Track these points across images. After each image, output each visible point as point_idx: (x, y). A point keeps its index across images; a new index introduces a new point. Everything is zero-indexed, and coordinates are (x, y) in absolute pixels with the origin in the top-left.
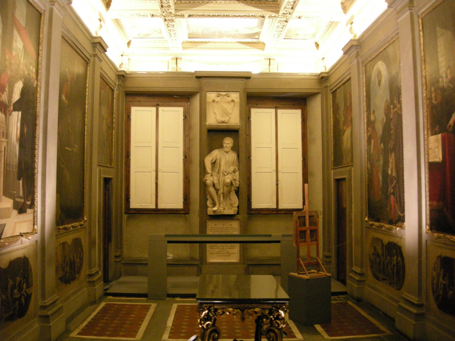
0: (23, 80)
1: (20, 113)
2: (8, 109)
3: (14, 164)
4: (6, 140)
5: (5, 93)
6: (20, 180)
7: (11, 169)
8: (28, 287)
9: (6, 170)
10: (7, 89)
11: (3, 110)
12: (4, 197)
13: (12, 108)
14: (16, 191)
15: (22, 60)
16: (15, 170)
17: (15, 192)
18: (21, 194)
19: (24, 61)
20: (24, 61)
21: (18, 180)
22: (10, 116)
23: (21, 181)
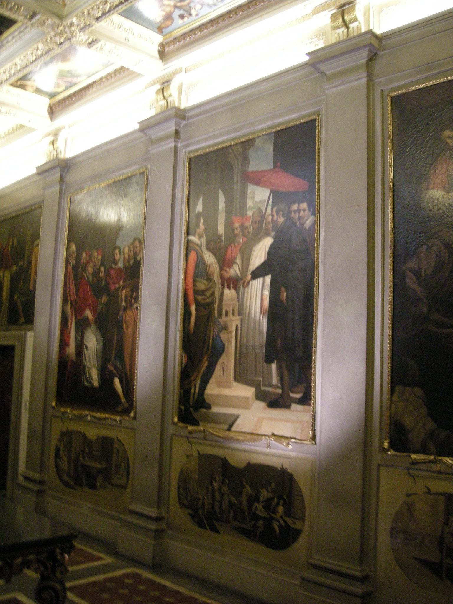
0: (273, 234)
1: (268, 279)
2: (242, 281)
3: (257, 343)
4: (238, 317)
5: (235, 267)
6: (273, 362)
7: (250, 350)
8: (288, 512)
9: (241, 352)
10: (238, 261)
11: (232, 286)
12: (235, 384)
13: (249, 277)
14: (263, 378)
15: (269, 211)
16: (258, 351)
17: (261, 379)
18: (275, 380)
19: (275, 209)
20: (275, 209)
21: (265, 364)
22: (246, 289)
23: (274, 366)
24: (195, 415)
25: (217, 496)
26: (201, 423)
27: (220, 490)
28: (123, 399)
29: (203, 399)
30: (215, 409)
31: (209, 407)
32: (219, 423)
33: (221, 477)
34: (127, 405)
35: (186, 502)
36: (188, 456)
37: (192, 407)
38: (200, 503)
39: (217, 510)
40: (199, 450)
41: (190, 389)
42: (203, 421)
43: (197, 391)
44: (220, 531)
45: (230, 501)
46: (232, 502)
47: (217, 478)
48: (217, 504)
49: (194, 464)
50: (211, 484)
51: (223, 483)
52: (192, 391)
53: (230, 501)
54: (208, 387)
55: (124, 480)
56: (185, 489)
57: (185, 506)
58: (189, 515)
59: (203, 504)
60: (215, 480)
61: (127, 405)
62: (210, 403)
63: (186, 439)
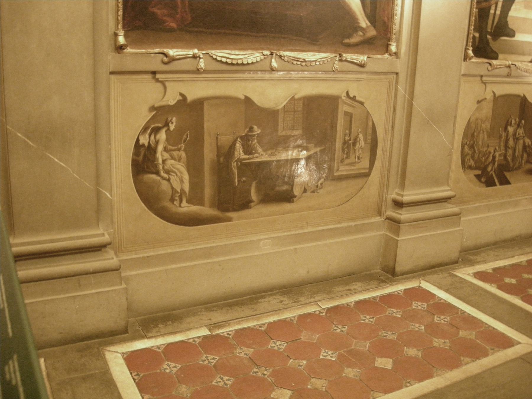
24: (494, 45)
25: (511, 142)
26: (500, 56)
27: (514, 134)
28: (364, 22)
29: (506, 23)
30: (519, 37)
31: (512, 34)
32: (523, 54)
33: (518, 120)
34: (372, 32)
35: (472, 163)
36: (479, 102)
37: (491, 34)
38: (491, 158)
39: (510, 159)
40: (495, 91)
41: (489, 8)
42: (504, 52)
43: (498, 12)
44: (511, 181)
45: (524, 143)
46: (527, 144)
47: (513, 122)
48: (510, 152)
49: (487, 110)
50: (506, 129)
51: (519, 126)
52: (492, 11)
53: (524, 143)
54: (514, 7)
55: (365, 163)
56: (472, 147)
57: (470, 168)
58: (474, 177)
59: (494, 157)
60: (511, 125)
61: (372, 32)
62: (514, 29)
63: (479, 78)
